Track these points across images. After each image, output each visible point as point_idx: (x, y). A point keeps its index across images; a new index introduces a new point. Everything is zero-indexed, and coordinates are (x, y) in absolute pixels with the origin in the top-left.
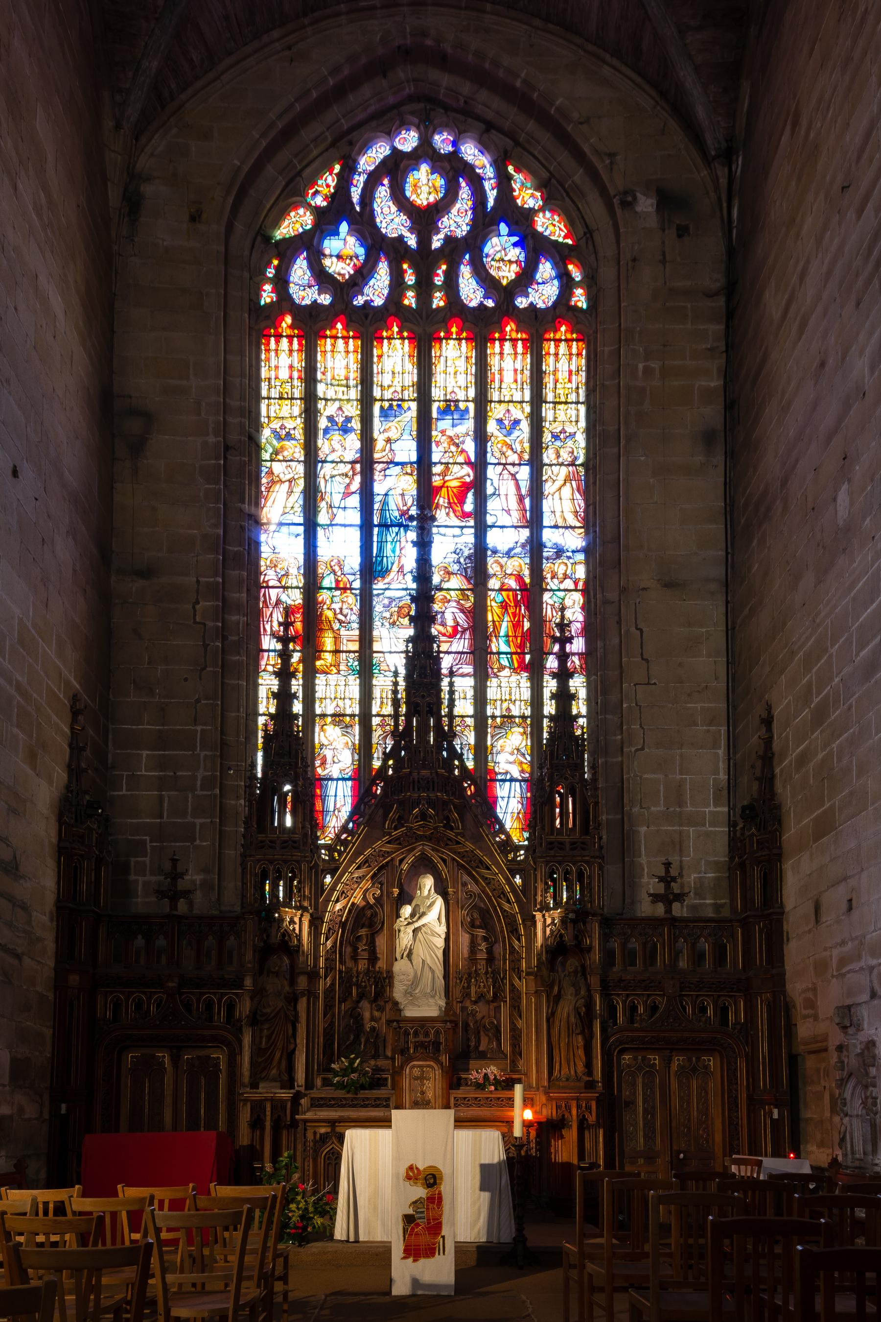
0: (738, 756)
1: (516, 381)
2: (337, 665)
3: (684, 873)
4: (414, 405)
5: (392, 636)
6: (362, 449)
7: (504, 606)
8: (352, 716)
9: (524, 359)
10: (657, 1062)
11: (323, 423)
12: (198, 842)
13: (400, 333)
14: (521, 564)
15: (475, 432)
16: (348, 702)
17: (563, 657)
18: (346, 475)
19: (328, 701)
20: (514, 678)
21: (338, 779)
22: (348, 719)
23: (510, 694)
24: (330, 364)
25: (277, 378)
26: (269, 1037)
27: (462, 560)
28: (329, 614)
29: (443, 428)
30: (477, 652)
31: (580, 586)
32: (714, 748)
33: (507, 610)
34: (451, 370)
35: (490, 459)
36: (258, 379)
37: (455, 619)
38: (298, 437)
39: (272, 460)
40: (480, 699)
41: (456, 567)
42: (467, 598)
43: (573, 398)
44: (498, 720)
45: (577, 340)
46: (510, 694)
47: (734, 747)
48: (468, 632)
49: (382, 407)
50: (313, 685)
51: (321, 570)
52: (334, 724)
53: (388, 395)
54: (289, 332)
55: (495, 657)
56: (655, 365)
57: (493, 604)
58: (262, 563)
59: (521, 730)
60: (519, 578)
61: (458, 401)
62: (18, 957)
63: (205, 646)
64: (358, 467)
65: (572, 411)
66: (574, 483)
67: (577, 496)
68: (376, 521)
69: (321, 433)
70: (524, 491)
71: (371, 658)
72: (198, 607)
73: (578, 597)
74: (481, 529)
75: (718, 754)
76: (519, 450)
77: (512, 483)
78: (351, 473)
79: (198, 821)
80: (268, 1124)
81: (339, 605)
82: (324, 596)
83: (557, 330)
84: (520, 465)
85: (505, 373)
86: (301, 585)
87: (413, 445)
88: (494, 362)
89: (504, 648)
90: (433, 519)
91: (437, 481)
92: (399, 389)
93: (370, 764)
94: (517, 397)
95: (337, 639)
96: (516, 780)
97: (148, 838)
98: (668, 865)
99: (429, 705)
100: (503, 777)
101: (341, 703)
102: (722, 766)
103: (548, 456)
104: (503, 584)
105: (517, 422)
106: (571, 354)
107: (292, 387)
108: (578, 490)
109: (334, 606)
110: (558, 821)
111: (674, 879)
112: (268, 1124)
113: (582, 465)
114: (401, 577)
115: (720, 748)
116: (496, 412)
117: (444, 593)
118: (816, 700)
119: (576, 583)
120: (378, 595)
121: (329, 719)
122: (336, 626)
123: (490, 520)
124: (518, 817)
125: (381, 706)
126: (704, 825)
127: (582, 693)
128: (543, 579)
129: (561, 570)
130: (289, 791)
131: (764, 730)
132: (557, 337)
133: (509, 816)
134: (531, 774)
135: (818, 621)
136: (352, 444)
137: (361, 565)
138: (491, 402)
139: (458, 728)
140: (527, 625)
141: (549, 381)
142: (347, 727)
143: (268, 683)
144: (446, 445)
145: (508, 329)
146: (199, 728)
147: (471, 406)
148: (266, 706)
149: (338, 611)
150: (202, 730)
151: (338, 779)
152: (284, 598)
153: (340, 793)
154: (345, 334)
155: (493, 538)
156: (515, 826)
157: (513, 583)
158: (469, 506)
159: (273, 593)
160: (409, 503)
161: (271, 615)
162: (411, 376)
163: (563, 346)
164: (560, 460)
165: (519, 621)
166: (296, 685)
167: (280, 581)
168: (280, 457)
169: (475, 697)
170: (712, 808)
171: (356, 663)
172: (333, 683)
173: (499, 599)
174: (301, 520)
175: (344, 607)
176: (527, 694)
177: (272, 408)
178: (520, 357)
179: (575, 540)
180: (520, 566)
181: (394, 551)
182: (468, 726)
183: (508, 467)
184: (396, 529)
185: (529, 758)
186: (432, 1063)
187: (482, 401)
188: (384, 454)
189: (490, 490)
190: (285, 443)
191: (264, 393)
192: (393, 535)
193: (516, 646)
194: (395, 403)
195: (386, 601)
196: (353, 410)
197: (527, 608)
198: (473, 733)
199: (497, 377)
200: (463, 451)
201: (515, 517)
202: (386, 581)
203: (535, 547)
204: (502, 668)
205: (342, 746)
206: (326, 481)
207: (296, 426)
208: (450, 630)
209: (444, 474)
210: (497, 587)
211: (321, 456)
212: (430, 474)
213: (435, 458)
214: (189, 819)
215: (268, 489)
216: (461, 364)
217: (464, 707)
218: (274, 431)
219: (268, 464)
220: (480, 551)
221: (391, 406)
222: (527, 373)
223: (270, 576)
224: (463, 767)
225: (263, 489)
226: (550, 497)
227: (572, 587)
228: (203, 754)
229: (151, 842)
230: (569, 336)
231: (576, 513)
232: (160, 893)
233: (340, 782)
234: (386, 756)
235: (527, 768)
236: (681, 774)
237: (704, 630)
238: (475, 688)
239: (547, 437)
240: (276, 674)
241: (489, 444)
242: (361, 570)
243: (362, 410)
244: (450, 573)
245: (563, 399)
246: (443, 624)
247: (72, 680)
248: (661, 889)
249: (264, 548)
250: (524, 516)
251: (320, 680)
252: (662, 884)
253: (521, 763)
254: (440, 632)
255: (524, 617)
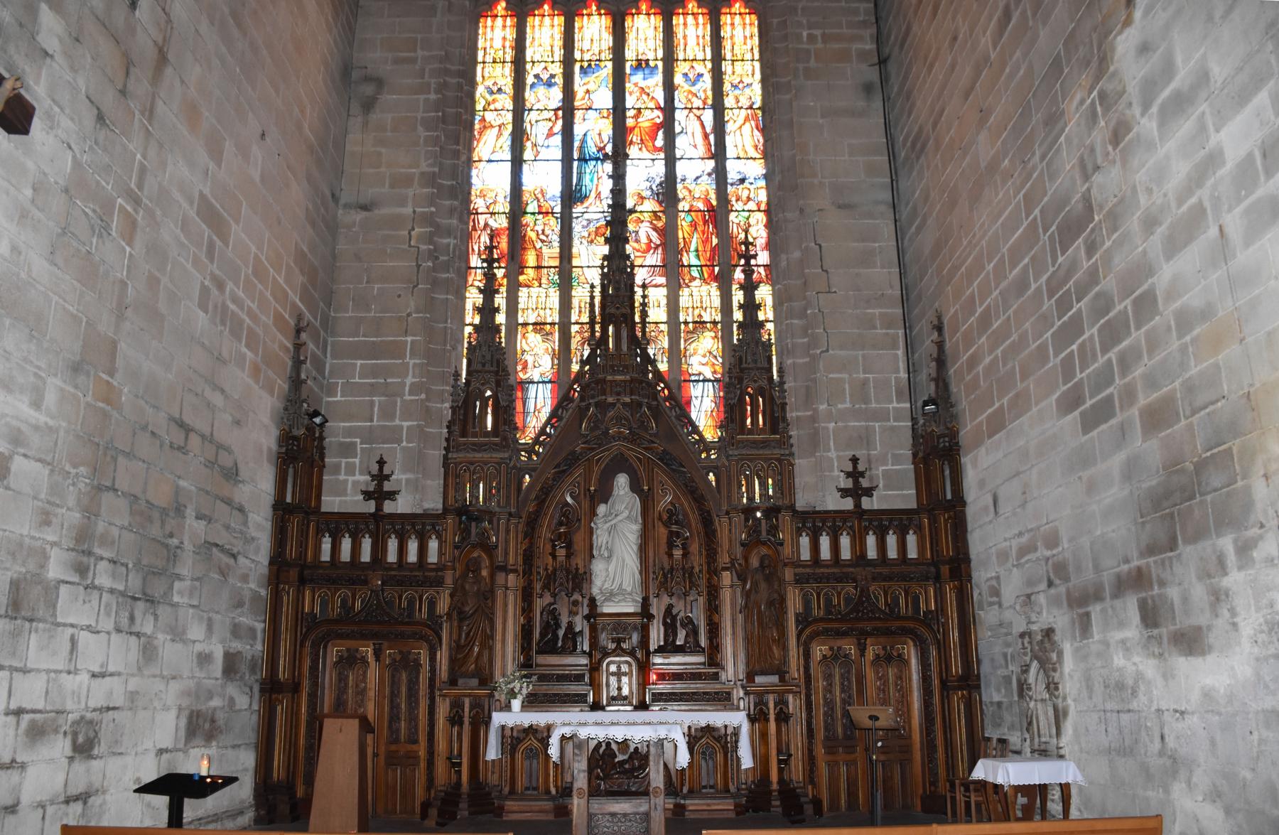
0: (916, 356)
1: (698, 44)
2: (539, 280)
3: (872, 466)
4: (610, 65)
5: (590, 252)
6: (563, 99)
7: (694, 225)
8: (552, 324)
9: (705, 28)
10: (853, 652)
11: (530, 80)
12: (404, 444)
13: (598, 9)
14: (707, 187)
15: (664, 84)
16: (548, 311)
17: (748, 272)
18: (550, 120)
19: (530, 311)
20: (705, 288)
21: (538, 383)
22: (548, 327)
23: (701, 302)
24: (537, 35)
25: (491, 47)
26: (468, 635)
27: (654, 187)
28: (533, 235)
29: (635, 81)
30: (668, 266)
31: (763, 207)
32: (893, 349)
33: (696, 229)
34: (641, 36)
35: (677, 104)
36: (475, 49)
37: (648, 237)
38: (508, 91)
39: (485, 110)
40: (673, 307)
41: (649, 193)
42: (659, 218)
43: (748, 56)
44: (691, 326)
45: (750, 14)
46: (701, 302)
47: (912, 348)
48: (660, 250)
49: (582, 67)
50: (517, 297)
51: (526, 197)
52: (535, 331)
53: (587, 57)
54: (503, 13)
55: (686, 270)
56: (818, 32)
57: (683, 223)
58: (473, 193)
59: (713, 334)
60: (707, 201)
61: (648, 60)
62: (234, 556)
63: (418, 266)
64: (560, 113)
65: (748, 65)
66: (753, 123)
67: (756, 133)
68: (576, 156)
69: (528, 88)
70: (708, 130)
71: (571, 272)
72: (413, 233)
73: (761, 217)
74: (671, 161)
75: (897, 355)
76: (703, 98)
77: (697, 123)
78: (553, 118)
79: (405, 424)
80: (466, 720)
81: (542, 227)
82: (528, 219)
83: (730, 6)
84: (704, 108)
85: (689, 39)
86: (507, 211)
87: (610, 94)
88: (679, 32)
89: (694, 261)
90: (626, 156)
91: (630, 122)
92: (597, 53)
93: (569, 368)
94: (700, 56)
95: (539, 256)
96: (709, 381)
97: (358, 440)
98: (855, 460)
99: (624, 315)
100: (697, 378)
101: (542, 313)
102: (902, 365)
103: (729, 102)
104: (692, 206)
105: (700, 75)
106: (744, 24)
107: (504, 53)
108: (757, 128)
109: (536, 228)
110: (749, 421)
111: (862, 474)
112: (466, 720)
113: (759, 108)
114: (598, 202)
115: (898, 349)
116: (681, 68)
117: (637, 215)
118: (979, 310)
119: (758, 205)
120: (577, 218)
121: (530, 328)
122: (539, 245)
123: (678, 154)
124: (711, 415)
125: (579, 315)
126: (889, 420)
127: (769, 301)
128: (728, 202)
129: (744, 195)
130: (490, 397)
131: (936, 334)
132: (733, 10)
133: (703, 415)
134: (723, 375)
135: (974, 242)
136: (555, 96)
137: (562, 192)
138: (677, 60)
139: (653, 334)
140: (715, 241)
141: (727, 45)
142: (547, 334)
143: (474, 297)
144: (638, 94)
145: (690, 6)
146: (409, 339)
147: (660, 64)
148: (472, 318)
149: (540, 232)
150: (413, 342)
151: (538, 383)
152: (491, 222)
153: (540, 395)
154: (551, 12)
155: (681, 169)
156: (709, 424)
157: (701, 206)
158: (660, 142)
159: (482, 219)
160: (606, 140)
161: (479, 237)
162: (608, 40)
163: (737, 18)
164: (740, 105)
165: (707, 238)
166: (500, 300)
167: (488, 208)
168: (492, 107)
169: (668, 305)
170: (895, 405)
171: (557, 277)
172: (534, 295)
173: (689, 219)
174: (509, 157)
175: (546, 228)
176: (717, 302)
177: (486, 70)
178: (701, 27)
179: (756, 169)
180: (707, 191)
181: (592, 181)
182: (662, 331)
183: (694, 111)
184: (594, 162)
185: (720, 360)
186: (628, 659)
187: (669, 60)
188: (583, 102)
189: (678, 129)
190: (497, 96)
191: (480, 59)
192: (592, 167)
193: (705, 259)
194: (593, 63)
195: (585, 223)
196: (557, 69)
197: (715, 227)
198: (667, 338)
199: (682, 41)
200: (653, 98)
201: (701, 150)
202: (586, 204)
203: (720, 174)
204: (693, 279)
205: (542, 352)
206: (532, 125)
207: (507, 83)
208: (644, 246)
209: (636, 117)
210: (686, 209)
211: (528, 105)
212: (624, 117)
213: (629, 104)
214: (397, 422)
215: (480, 133)
216: (651, 33)
217: (658, 314)
218: (488, 88)
219: (481, 113)
220: (670, 179)
221: (590, 65)
222: (708, 38)
223: (479, 204)
224: (657, 373)
225: (476, 133)
226: (732, 134)
227: (756, 208)
228: (412, 362)
229: (361, 444)
230: (743, 11)
231: (756, 147)
232: (368, 495)
233: (540, 385)
234: (583, 363)
235: (719, 369)
236: (865, 372)
237: (877, 245)
238: (668, 297)
239: (727, 87)
240: (481, 291)
241: (676, 93)
242: (562, 197)
243: (564, 69)
244: (643, 198)
245: (739, 58)
246: (637, 241)
247: (297, 301)
248: (848, 484)
249: (474, 180)
250: (709, 150)
251: (523, 293)
252: (850, 480)
253: (714, 364)
254: (634, 249)
255: (712, 234)
